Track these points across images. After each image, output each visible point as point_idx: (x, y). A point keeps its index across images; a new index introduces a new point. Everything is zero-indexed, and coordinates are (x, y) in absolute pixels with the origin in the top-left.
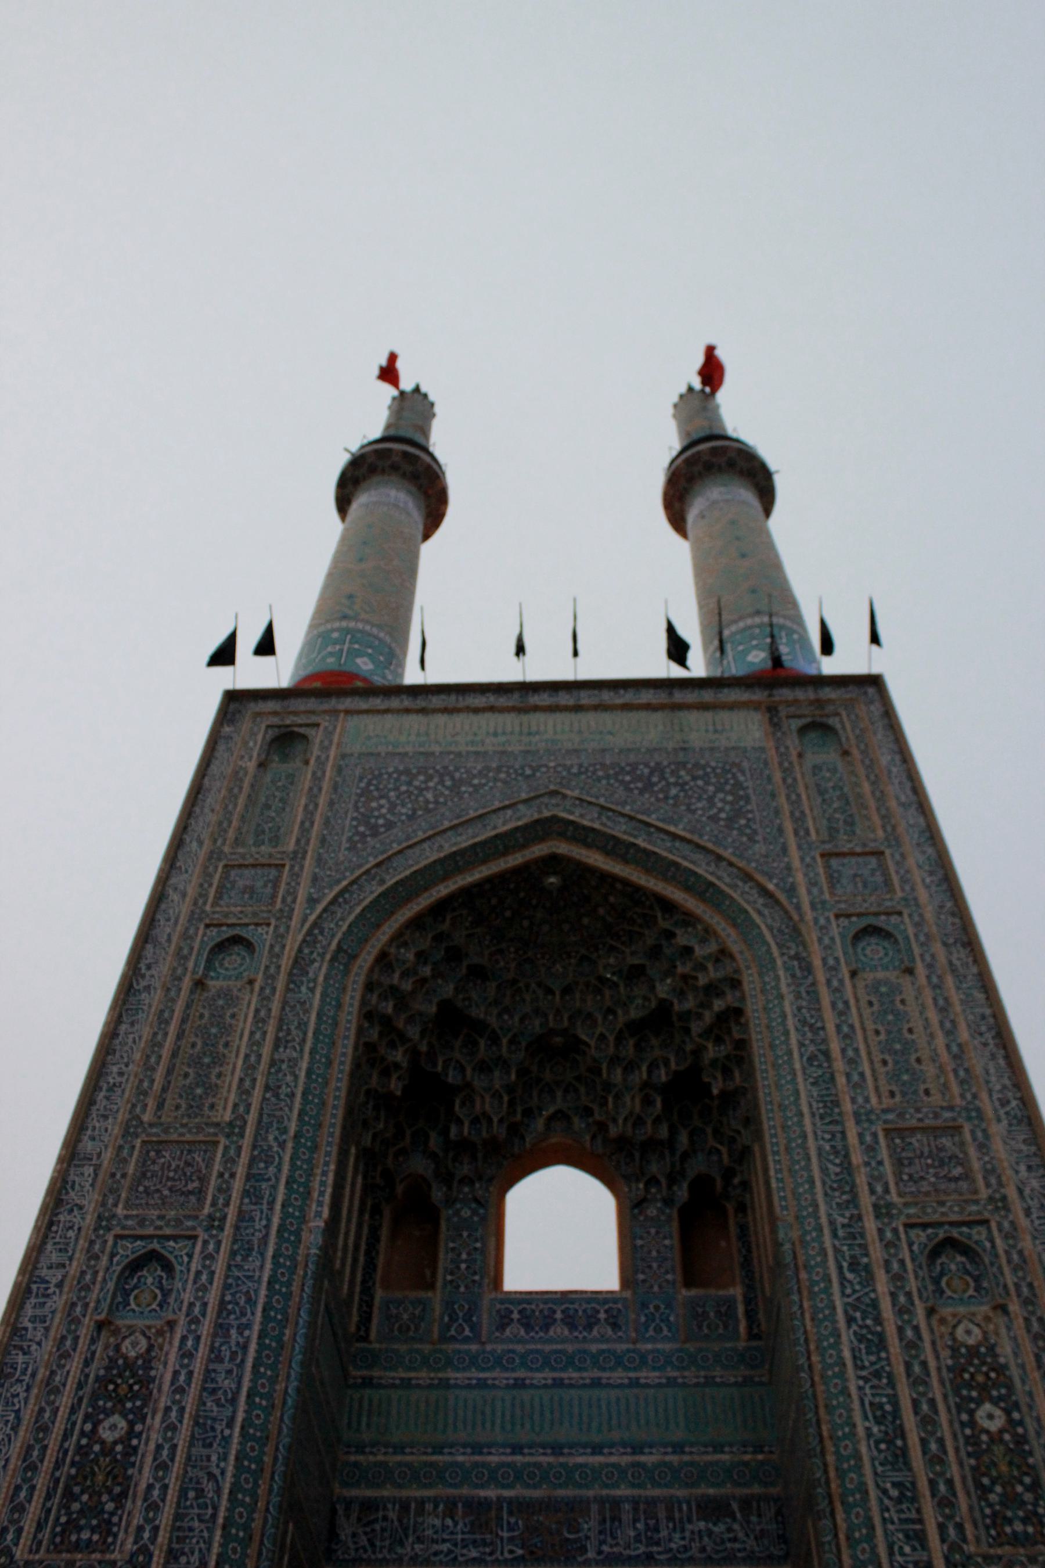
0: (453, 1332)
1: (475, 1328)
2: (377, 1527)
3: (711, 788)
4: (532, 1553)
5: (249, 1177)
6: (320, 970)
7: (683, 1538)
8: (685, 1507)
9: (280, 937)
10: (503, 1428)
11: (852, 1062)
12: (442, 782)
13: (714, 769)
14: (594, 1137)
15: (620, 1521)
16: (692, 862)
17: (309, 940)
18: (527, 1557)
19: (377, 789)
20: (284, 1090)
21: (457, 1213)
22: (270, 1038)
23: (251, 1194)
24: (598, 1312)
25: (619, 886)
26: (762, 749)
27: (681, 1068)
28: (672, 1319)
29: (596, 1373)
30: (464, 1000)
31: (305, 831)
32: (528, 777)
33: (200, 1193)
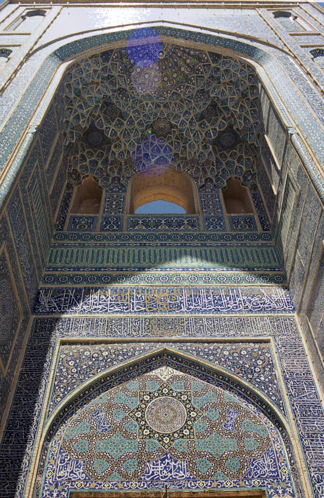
0: (108, 227)
1: (120, 228)
2: (63, 299)
4: (150, 309)
7: (236, 303)
8: (235, 291)
10: (134, 261)
14: (179, 165)
15: (199, 296)
18: (147, 310)
24: (184, 221)
25: (192, 52)
27: (223, 130)
28: (222, 224)
29: (183, 242)
30: (117, 102)
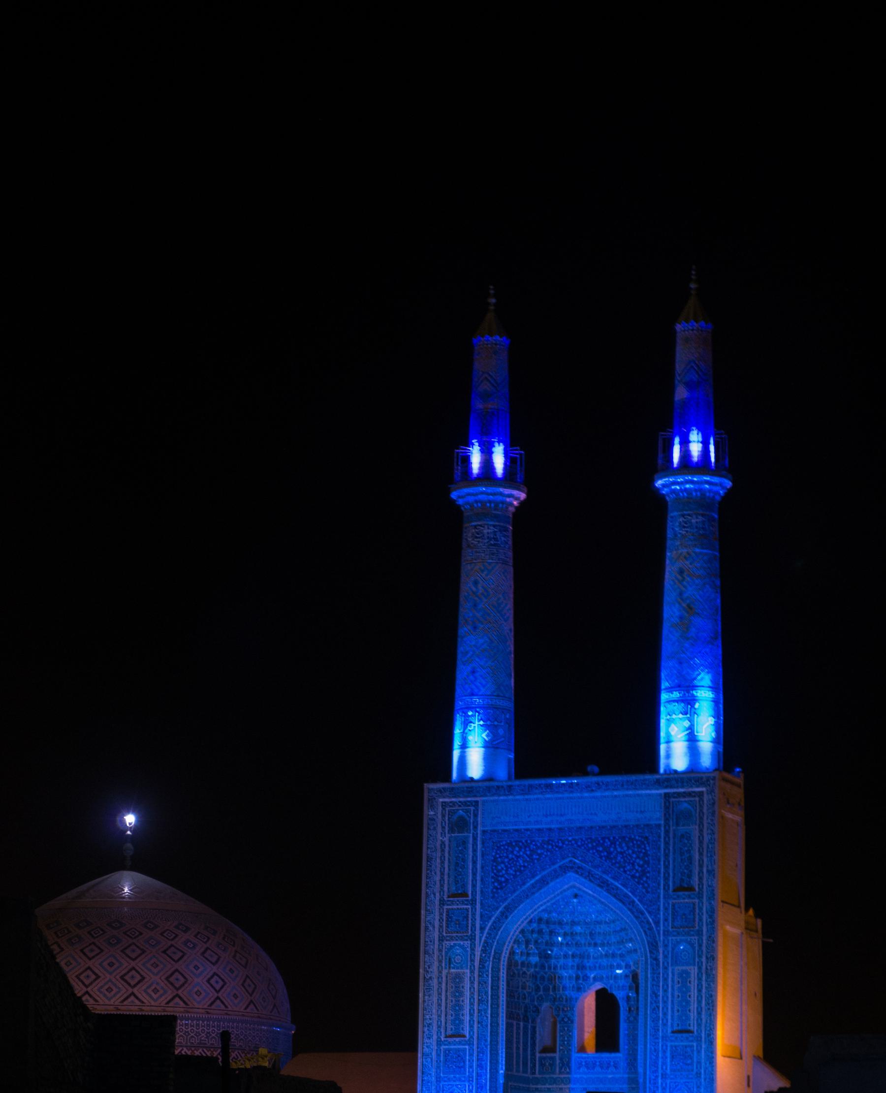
3: (634, 856)
5: (478, 1060)
6: (489, 965)
9: (473, 949)
11: (665, 1014)
12: (524, 853)
13: (637, 841)
16: (623, 903)
17: (484, 951)
19: (500, 857)
20: (484, 1023)
21: (563, 1019)
22: (476, 1001)
23: (480, 1066)
26: (659, 826)
31: (474, 886)
32: (560, 848)
33: (464, 1067)
